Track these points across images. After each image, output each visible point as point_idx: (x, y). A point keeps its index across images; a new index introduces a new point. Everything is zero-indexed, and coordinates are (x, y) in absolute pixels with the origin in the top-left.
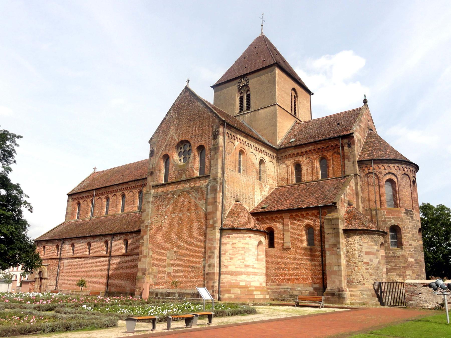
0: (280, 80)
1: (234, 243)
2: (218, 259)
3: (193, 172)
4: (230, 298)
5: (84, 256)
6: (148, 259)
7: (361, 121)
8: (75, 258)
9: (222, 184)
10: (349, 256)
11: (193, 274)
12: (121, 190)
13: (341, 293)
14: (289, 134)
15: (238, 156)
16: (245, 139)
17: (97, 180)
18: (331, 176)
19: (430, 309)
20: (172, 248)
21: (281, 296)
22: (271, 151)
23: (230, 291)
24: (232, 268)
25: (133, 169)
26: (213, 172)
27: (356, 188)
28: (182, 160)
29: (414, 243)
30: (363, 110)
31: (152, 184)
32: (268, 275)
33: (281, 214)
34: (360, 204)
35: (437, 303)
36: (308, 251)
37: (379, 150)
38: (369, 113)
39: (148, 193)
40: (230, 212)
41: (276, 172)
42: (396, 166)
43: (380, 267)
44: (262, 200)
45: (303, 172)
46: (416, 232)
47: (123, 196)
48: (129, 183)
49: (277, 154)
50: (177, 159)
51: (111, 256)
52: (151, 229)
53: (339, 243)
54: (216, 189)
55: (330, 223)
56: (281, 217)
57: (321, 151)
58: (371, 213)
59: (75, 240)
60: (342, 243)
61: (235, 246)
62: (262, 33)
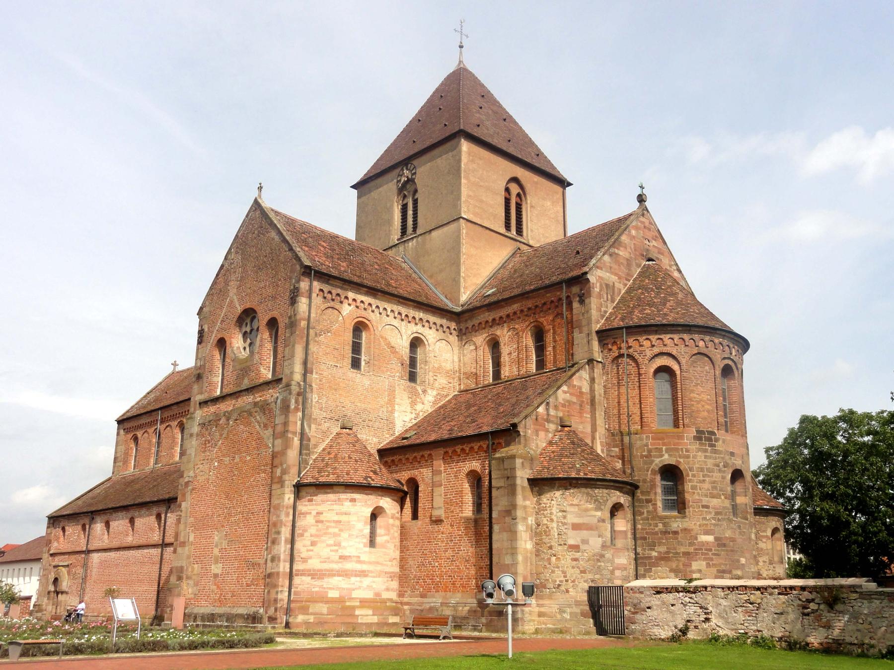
2: (289, 546)
3: (258, 373)
4: (307, 623)
6: (187, 548)
9: (302, 394)
10: (539, 534)
11: (250, 575)
14: (494, 276)
15: (349, 337)
16: (367, 299)
18: (550, 366)
19: (663, 640)
20: (223, 526)
23: (308, 608)
24: (314, 564)
27: (592, 390)
28: (248, 349)
29: (715, 502)
30: (632, 217)
32: (403, 577)
33: (430, 450)
35: (676, 627)
37: (649, 305)
38: (652, 223)
40: (324, 450)
41: (456, 359)
42: (676, 337)
43: (608, 555)
44: (414, 422)
46: (723, 478)
49: (458, 323)
50: (238, 348)
52: (193, 489)
53: (514, 506)
54: (288, 406)
56: (430, 455)
57: (534, 314)
58: (622, 440)
59: (111, 514)
60: (525, 507)
61: (322, 518)
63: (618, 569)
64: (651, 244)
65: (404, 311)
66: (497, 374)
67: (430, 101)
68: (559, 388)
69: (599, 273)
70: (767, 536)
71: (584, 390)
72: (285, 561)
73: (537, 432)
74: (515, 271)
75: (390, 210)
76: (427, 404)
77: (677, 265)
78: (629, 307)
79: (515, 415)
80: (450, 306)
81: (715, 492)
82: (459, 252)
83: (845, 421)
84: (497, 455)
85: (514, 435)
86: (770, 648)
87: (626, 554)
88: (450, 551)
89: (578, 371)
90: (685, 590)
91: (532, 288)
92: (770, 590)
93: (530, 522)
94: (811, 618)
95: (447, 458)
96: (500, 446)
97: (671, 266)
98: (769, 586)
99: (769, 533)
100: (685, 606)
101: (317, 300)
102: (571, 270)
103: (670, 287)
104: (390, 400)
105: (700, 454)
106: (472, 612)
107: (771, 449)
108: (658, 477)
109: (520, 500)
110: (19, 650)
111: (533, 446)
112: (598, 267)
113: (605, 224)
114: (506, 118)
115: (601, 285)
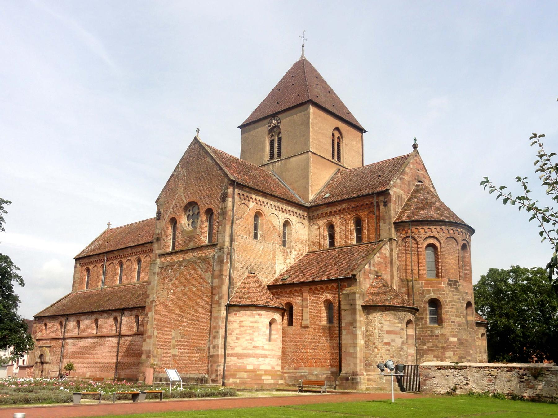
1: (241, 322)
2: (224, 340)
3: (200, 240)
4: (235, 383)
5: (91, 335)
6: (152, 340)
7: (403, 173)
8: (81, 338)
9: (230, 254)
10: (368, 336)
11: (198, 356)
12: (136, 253)
13: (355, 377)
14: (327, 186)
15: (252, 220)
16: (262, 199)
17: (110, 239)
18: (365, 240)
19: (442, 394)
20: (178, 327)
21: (298, 381)
22: (300, 210)
24: (238, 350)
25: (152, 227)
26: (220, 240)
27: (391, 256)
29: (458, 320)
30: (410, 157)
31: (159, 252)
32: (284, 357)
33: (301, 287)
34: (395, 273)
35: (449, 388)
36: (327, 330)
37: (422, 208)
38: (421, 160)
39: (153, 263)
40: (240, 285)
41: (307, 234)
42: (438, 228)
43: (405, 348)
44: (285, 270)
45: (336, 235)
46: (462, 306)
47: (139, 261)
48: (146, 245)
49: (308, 213)
50: (185, 224)
51: (120, 336)
52: (156, 305)
53: (355, 320)
54: (223, 260)
55: (347, 299)
56: (300, 290)
58: (408, 284)
59: (81, 316)
60: (360, 321)
62: (303, 56)
63: (409, 357)
64: (420, 172)
65: (281, 206)
66: (332, 243)
67: (285, 78)
68: (375, 255)
69: (395, 189)
72: (221, 348)
73: (365, 279)
75: (263, 143)
76: (292, 260)
77: (432, 184)
78: (411, 209)
79: (352, 270)
80: (303, 202)
82: (309, 171)
83: (514, 273)
84: (344, 292)
85: (354, 281)
86: (502, 399)
88: (313, 344)
89: (384, 245)
90: (455, 368)
91: (355, 195)
92: (502, 369)
94: (524, 383)
95: (311, 292)
96: (344, 287)
97: (429, 185)
98: (502, 367)
99: (480, 336)
100: (455, 376)
101: (237, 199)
102: (379, 187)
103: (432, 198)
106: (328, 378)
108: (427, 305)
109: (358, 317)
110: (145, 396)
112: (394, 186)
113: (393, 159)
114: (330, 91)
115: (396, 197)
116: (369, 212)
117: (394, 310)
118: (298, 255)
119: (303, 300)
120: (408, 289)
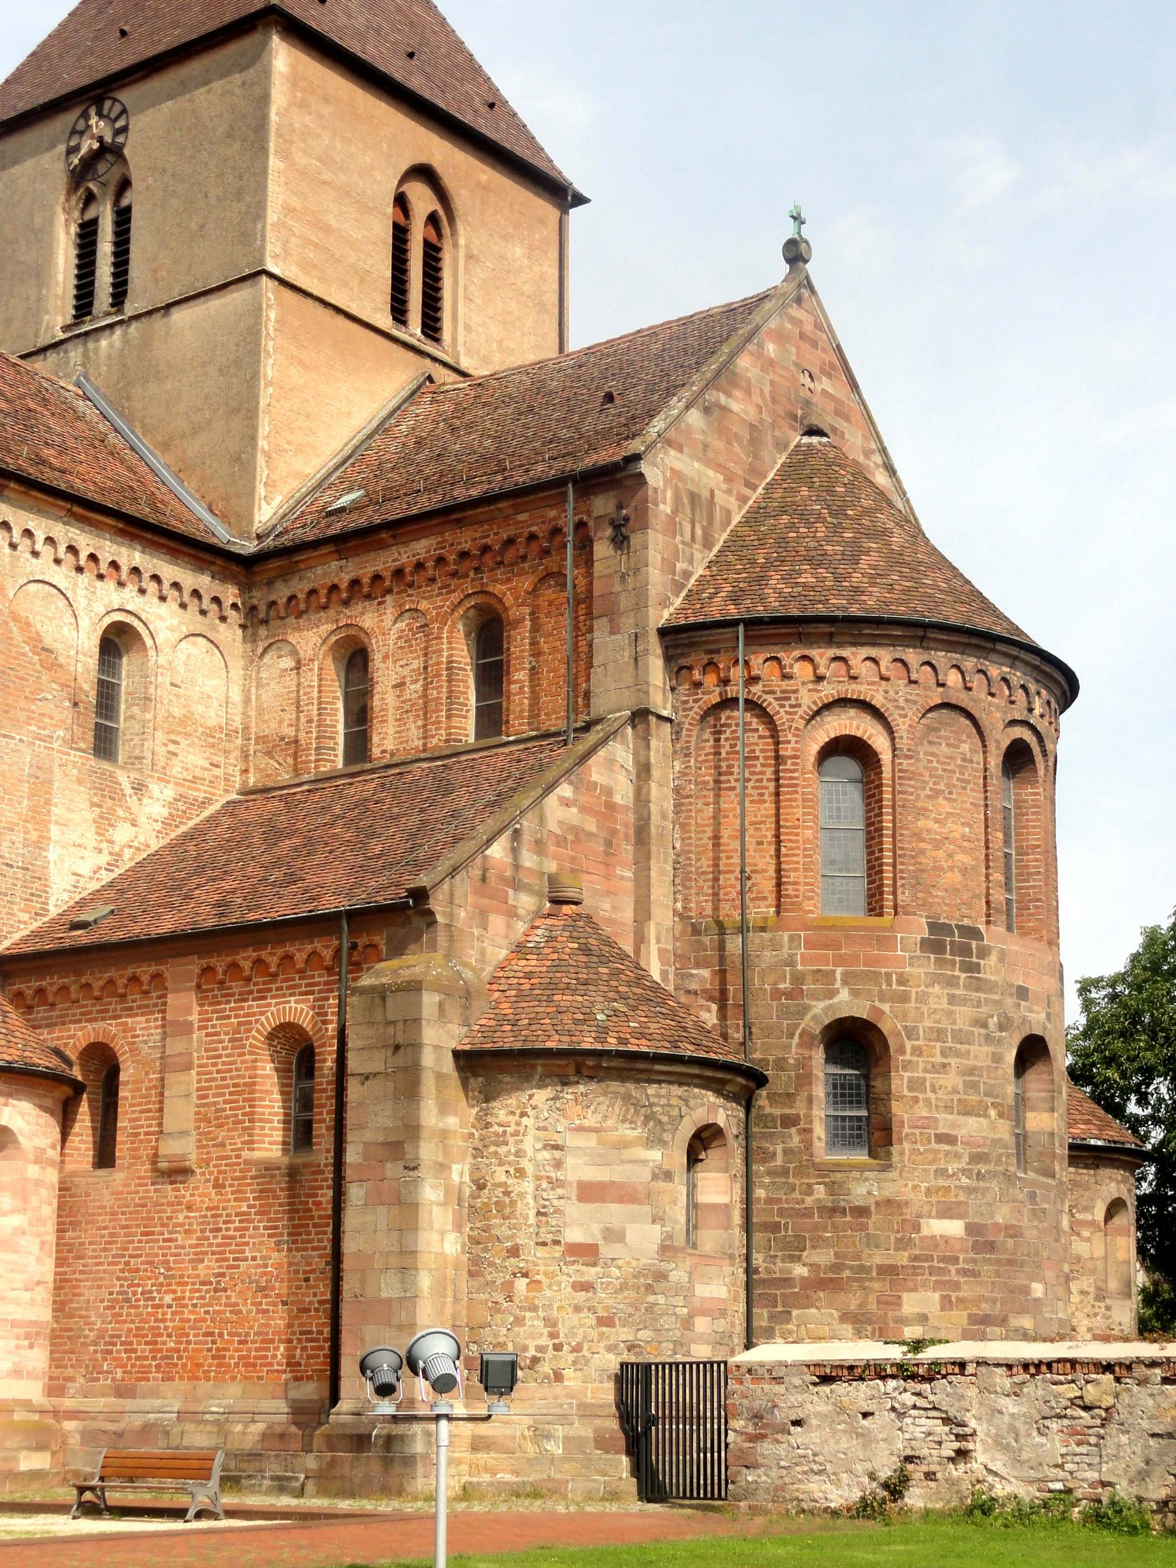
0: (302, 120)
7: (725, 377)
10: (482, 1210)
13: (401, 1429)
14: (353, 456)
18: (518, 724)
19: (835, 1513)
27: (641, 799)
29: (971, 1127)
30: (768, 305)
32: (64, 1337)
33: (160, 960)
34: (661, 890)
35: (872, 1476)
36: (280, 1185)
37: (810, 560)
38: (823, 325)
41: (236, 695)
42: (885, 655)
43: (678, 1275)
44: (106, 877)
45: (376, 702)
46: (997, 1058)
49: (246, 587)
53: (413, 1130)
56: (157, 976)
57: (477, 570)
58: (722, 947)
60: (444, 1134)
63: (700, 1312)
65: (86, 541)
68: (549, 789)
69: (673, 459)
70: (1093, 1223)
71: (617, 799)
73: (482, 917)
74: (419, 442)
75: (42, 237)
77: (883, 451)
78: (753, 562)
79: (419, 866)
80: (222, 534)
81: (973, 1098)
82: (256, 376)
84: (366, 981)
85: (418, 922)
86: (1133, 1531)
87: (727, 1269)
88: (210, 1262)
89: (603, 742)
90: (904, 1372)
91: (475, 492)
92: (1140, 1371)
93: (455, 1177)
95: (210, 986)
96: (373, 953)
97: (867, 453)
98: (1139, 1361)
99: (1099, 1213)
100: (901, 1415)
102: (593, 448)
103: (866, 512)
104: (33, 809)
105: (936, 989)
106: (275, 1438)
107: (1096, 983)
108: (819, 1055)
109: (429, 1114)
111: (471, 956)
112: (669, 443)
115: (677, 499)
116: (542, 580)
117: (622, 1075)
118: (183, 804)
119: (169, 1029)
120: (723, 973)
